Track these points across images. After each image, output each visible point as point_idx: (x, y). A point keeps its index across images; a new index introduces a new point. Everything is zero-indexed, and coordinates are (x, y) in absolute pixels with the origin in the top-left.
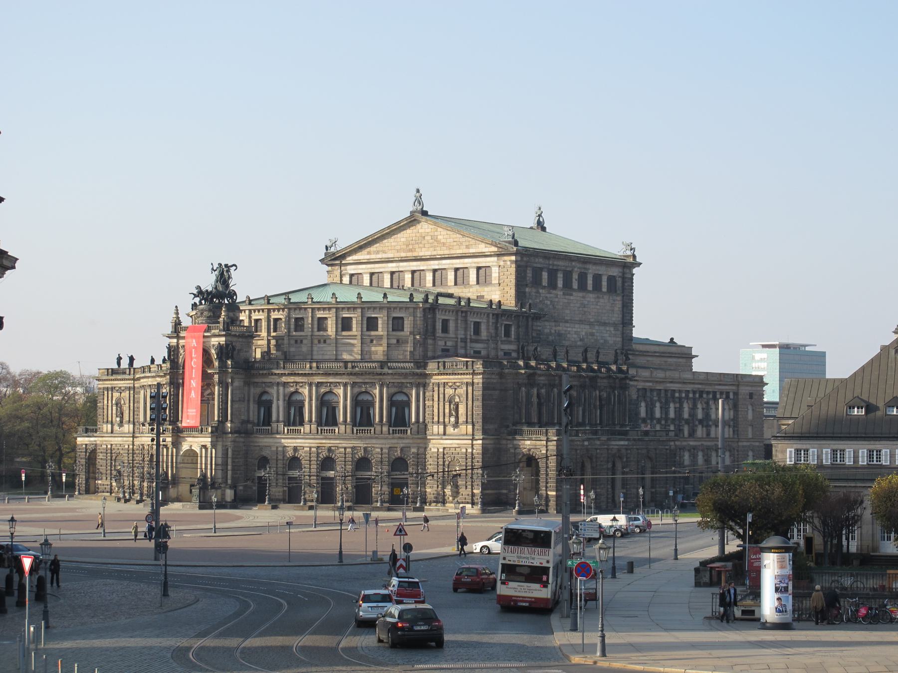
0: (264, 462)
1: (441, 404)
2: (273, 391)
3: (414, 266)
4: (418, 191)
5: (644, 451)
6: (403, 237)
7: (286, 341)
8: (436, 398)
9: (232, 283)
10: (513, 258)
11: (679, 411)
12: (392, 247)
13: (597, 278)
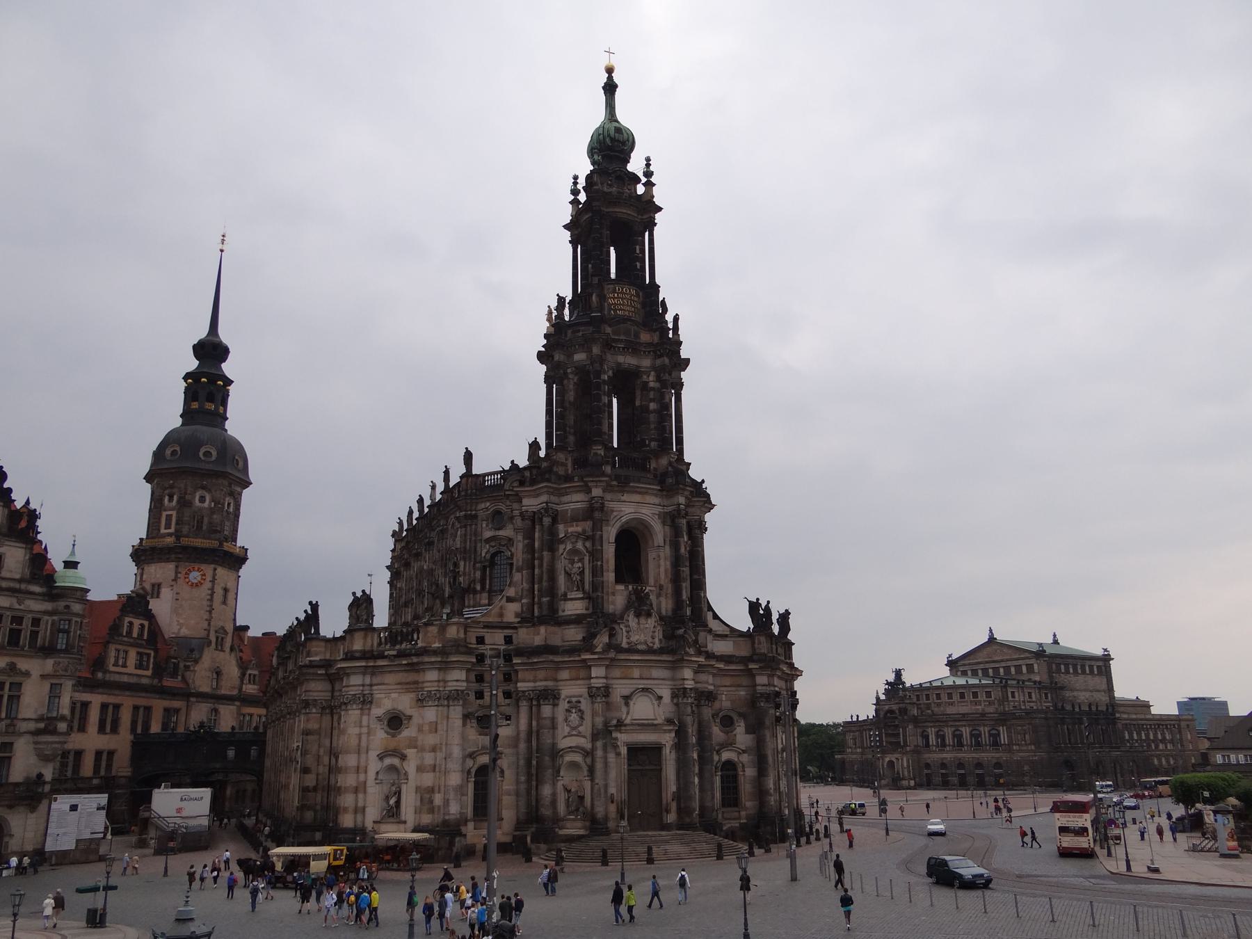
0: (928, 766)
6: (985, 652)
11: (1147, 735)
12: (981, 657)
13: (1091, 667)
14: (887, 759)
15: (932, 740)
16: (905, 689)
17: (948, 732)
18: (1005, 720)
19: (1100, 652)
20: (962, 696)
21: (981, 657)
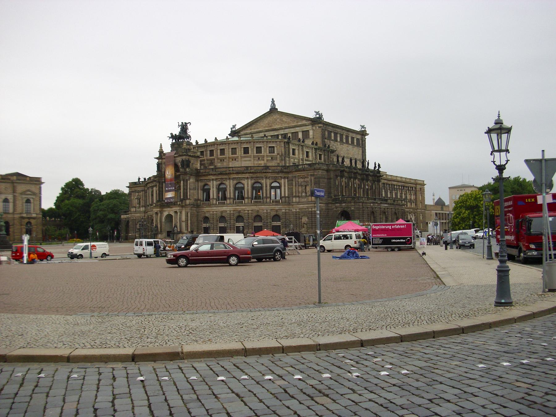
0: (206, 219)
1: (297, 186)
2: (211, 184)
3: (272, 133)
4: (273, 99)
5: (394, 210)
6: (266, 121)
7: (216, 161)
8: (294, 184)
9: (188, 131)
10: (320, 125)
11: (396, 194)
12: (262, 126)
14: (165, 214)
15: (213, 193)
16: (190, 144)
17: (230, 185)
18: (288, 173)
19: (358, 129)
20: (246, 151)
21: (262, 126)
